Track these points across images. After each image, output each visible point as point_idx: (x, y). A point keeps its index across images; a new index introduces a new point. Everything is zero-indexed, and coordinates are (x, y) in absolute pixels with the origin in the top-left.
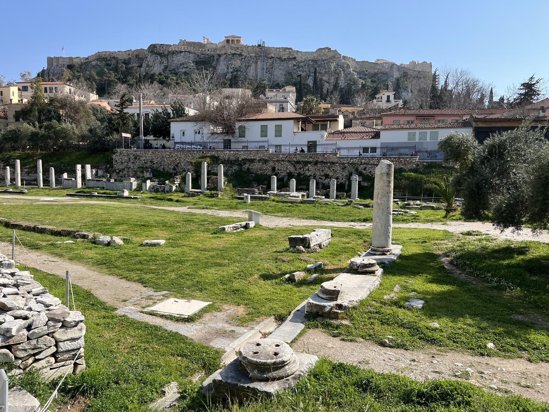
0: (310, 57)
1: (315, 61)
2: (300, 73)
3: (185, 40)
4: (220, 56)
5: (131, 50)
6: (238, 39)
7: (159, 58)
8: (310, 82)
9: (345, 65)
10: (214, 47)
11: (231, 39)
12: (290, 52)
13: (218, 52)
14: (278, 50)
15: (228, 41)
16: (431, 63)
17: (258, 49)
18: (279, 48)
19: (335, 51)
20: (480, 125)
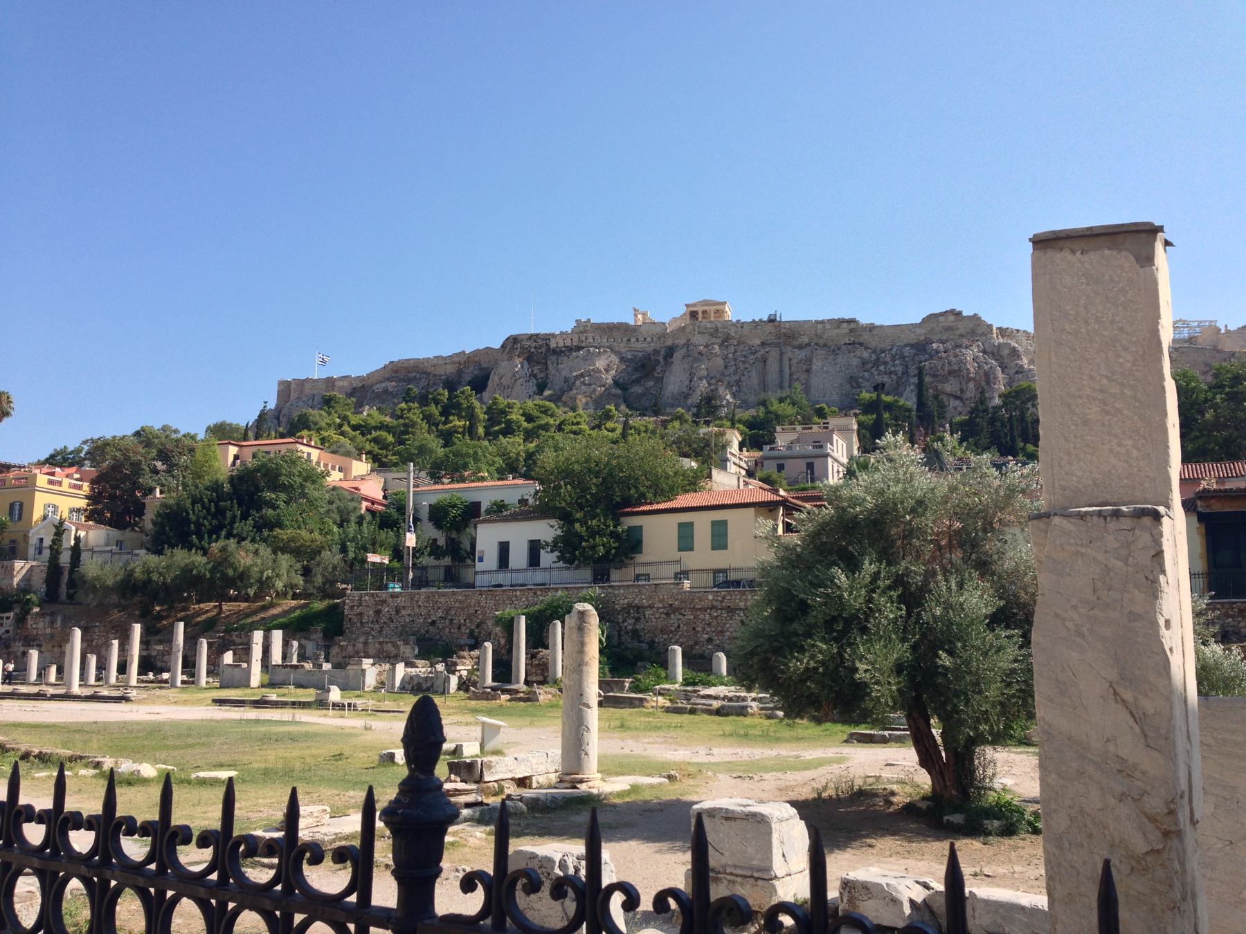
0: (911, 338)
1: (921, 347)
2: (879, 379)
3: (589, 320)
4: (671, 351)
5: (463, 352)
9: (1006, 352)
10: (658, 330)
11: (700, 309)
12: (851, 330)
13: (669, 343)
14: (820, 326)
15: (693, 315)
17: (769, 328)
18: (822, 322)
19: (975, 318)
20: (1217, 507)
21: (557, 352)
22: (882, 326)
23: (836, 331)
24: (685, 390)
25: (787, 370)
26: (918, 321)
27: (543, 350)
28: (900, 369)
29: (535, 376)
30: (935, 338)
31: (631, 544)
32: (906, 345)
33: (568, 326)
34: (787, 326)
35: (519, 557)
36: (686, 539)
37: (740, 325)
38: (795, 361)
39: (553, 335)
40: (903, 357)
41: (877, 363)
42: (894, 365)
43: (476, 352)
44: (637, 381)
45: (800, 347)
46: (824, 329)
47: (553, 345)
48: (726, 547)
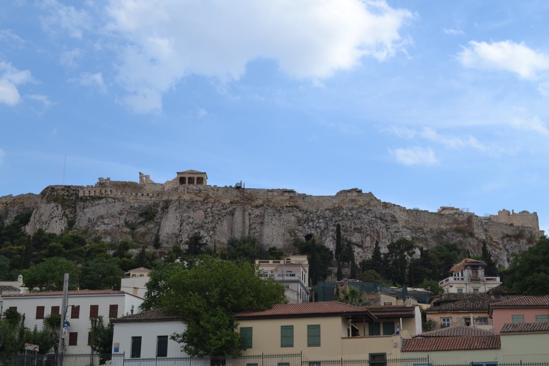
0: (329, 205)
1: (336, 211)
2: (309, 232)
3: (108, 179)
5: (10, 196)
6: (200, 176)
7: (60, 209)
8: (330, 245)
10: (158, 189)
12: (291, 197)
13: (165, 198)
14: (270, 194)
15: (182, 180)
16: (535, 213)
17: (235, 192)
18: (272, 191)
21: (84, 200)
22: (311, 196)
23: (281, 198)
24: (177, 232)
25: (247, 222)
26: (334, 194)
27: (73, 198)
28: (323, 225)
29: (67, 216)
30: (345, 207)
31: (246, 341)
32: (326, 210)
33: (93, 182)
34: (249, 191)
35: (149, 348)
36: (287, 338)
37: (216, 189)
38: (252, 216)
39: (82, 188)
40: (324, 218)
41: (307, 221)
42: (319, 223)
43: (21, 197)
44: (142, 223)
45: (257, 207)
46: (273, 196)
47: (81, 194)
48: (318, 345)
